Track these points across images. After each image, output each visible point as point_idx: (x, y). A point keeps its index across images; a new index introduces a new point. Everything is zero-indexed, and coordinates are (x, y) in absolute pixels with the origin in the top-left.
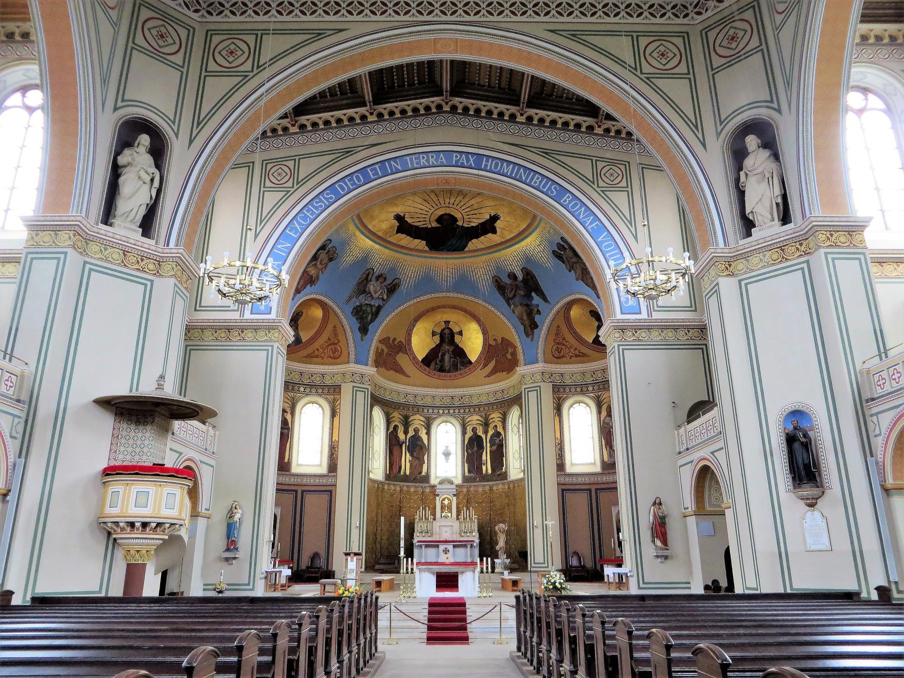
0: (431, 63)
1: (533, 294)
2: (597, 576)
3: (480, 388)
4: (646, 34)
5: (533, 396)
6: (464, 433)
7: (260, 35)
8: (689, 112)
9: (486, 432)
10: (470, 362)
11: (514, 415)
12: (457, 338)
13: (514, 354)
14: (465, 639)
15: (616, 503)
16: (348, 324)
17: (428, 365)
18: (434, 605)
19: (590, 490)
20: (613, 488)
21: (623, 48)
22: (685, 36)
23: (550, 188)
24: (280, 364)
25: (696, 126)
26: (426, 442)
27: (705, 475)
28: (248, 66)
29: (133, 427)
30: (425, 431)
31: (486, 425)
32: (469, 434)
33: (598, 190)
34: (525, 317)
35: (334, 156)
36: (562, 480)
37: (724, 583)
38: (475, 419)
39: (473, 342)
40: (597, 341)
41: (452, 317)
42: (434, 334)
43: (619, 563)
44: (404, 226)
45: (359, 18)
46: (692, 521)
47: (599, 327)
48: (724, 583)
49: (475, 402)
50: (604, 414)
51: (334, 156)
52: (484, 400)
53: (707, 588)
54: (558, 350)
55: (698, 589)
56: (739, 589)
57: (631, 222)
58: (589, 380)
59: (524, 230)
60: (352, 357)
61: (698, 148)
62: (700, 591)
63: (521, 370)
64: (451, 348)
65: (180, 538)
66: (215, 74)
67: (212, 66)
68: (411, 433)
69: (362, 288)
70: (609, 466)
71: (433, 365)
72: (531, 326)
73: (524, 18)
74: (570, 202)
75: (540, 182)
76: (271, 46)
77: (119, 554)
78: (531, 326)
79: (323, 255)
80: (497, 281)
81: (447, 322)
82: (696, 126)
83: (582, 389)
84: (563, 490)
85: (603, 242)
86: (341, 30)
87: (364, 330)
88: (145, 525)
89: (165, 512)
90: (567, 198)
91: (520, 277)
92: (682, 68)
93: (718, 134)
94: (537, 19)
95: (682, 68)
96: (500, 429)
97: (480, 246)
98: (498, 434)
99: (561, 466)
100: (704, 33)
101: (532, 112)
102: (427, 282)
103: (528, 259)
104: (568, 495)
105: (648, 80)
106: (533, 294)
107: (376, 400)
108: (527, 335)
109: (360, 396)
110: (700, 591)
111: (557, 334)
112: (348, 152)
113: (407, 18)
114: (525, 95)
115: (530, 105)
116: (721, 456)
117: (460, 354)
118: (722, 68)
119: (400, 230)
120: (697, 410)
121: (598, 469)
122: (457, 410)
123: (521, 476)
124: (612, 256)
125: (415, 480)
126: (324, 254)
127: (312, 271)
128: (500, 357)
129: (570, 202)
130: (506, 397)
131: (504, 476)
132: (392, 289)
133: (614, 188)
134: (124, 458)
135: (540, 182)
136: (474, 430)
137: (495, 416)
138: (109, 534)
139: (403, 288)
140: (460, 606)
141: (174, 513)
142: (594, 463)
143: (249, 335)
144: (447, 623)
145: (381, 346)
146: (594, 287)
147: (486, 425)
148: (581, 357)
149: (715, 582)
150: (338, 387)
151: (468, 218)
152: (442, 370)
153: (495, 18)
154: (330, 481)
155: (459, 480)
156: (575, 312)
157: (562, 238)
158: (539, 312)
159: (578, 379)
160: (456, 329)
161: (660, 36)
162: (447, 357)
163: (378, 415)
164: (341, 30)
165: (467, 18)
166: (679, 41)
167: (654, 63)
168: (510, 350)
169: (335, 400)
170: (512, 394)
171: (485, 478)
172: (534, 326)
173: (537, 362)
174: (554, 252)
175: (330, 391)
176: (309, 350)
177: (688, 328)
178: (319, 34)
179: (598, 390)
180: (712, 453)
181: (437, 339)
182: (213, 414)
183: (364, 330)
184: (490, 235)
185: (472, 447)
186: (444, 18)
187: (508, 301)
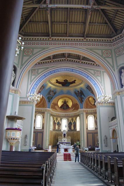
0: (63, 53)
2: (94, 150)
3: (72, 113)
4: (104, 49)
5: (82, 115)
6: (68, 122)
7: (33, 48)
8: (112, 64)
9: (72, 121)
10: (69, 108)
11: (78, 118)
12: (67, 103)
13: (78, 106)
14: (71, 160)
15: (98, 136)
16: (47, 100)
17: (61, 108)
18: (65, 155)
19: (93, 133)
20: (97, 133)
21: (99, 52)
22: (111, 50)
24: (34, 108)
25: (113, 67)
26: (60, 123)
27: (114, 131)
28: (31, 55)
29: (10, 121)
30: (60, 121)
31: (72, 120)
32: (69, 122)
34: (80, 99)
35: (44, 69)
36: (87, 131)
37: (117, 151)
38: (70, 119)
39: (70, 104)
40: (94, 104)
41: (67, 99)
42: (62, 102)
43: (98, 147)
44: (57, 82)
45: (51, 46)
46: (112, 139)
47: (95, 102)
48: (117, 151)
49: (70, 115)
50: (96, 118)
51: (44, 69)
52: (72, 115)
53: (114, 152)
54: (87, 106)
55: (112, 151)
56: (119, 152)
57: (101, 82)
58: (93, 112)
60: (47, 106)
61: (113, 71)
62: (113, 152)
63: (80, 110)
64: (66, 105)
65: (19, 141)
66: (25, 56)
67: (25, 54)
68: (58, 121)
69: (49, 93)
70: (96, 129)
71: (62, 108)
72: (82, 101)
76: (35, 51)
77: (9, 144)
78: (82, 101)
79: (42, 87)
81: (65, 100)
82: (113, 67)
83: (91, 114)
84: (87, 133)
86: (48, 48)
87: (49, 101)
88: (14, 139)
89: (17, 136)
91: (80, 92)
92: (110, 56)
93: (117, 69)
94: (84, 46)
95: (110, 56)
96: (75, 121)
97: (72, 86)
98: (75, 122)
99: (87, 129)
100: (115, 49)
101: (82, 61)
102: (62, 92)
103: (81, 88)
104: (88, 134)
105: (104, 58)
107: (51, 115)
108: (81, 103)
109: (48, 114)
110: (113, 152)
111: (87, 103)
112: (48, 68)
113: (60, 46)
115: (82, 60)
116: (117, 128)
117: (68, 106)
118: (117, 57)
119: (57, 82)
120: (113, 118)
121: (94, 129)
122: (67, 117)
123: (79, 130)
125: (58, 131)
126: (43, 87)
127: (40, 90)
128: (75, 107)
130: (77, 114)
131: (76, 130)
132: (55, 93)
133: (98, 76)
134: (9, 127)
136: (70, 121)
137: (74, 118)
138: (7, 140)
139: (57, 94)
140: (69, 155)
141: (19, 137)
142: (93, 128)
143: (29, 103)
144: (67, 157)
145: (53, 104)
146: (94, 94)
147: (72, 120)
148: (91, 107)
149: (115, 151)
150: (44, 112)
151: (70, 80)
152: (64, 109)
154: (43, 131)
155: (67, 131)
156: (90, 99)
157: (88, 85)
159: (91, 112)
160: (67, 101)
161: (107, 50)
162: (65, 106)
163: (51, 118)
164: (48, 48)
166: (110, 51)
167: (105, 55)
168: (77, 105)
169: (43, 115)
170: (78, 114)
171: (72, 130)
172: (82, 101)
173: (83, 108)
174: (86, 87)
175: (42, 113)
176: (39, 105)
177: (112, 103)
178: (44, 49)
179: (94, 114)
180: (115, 127)
181: (63, 103)
182: (25, 119)
183: (49, 101)
184: (74, 84)
185: (70, 125)
187: (77, 96)
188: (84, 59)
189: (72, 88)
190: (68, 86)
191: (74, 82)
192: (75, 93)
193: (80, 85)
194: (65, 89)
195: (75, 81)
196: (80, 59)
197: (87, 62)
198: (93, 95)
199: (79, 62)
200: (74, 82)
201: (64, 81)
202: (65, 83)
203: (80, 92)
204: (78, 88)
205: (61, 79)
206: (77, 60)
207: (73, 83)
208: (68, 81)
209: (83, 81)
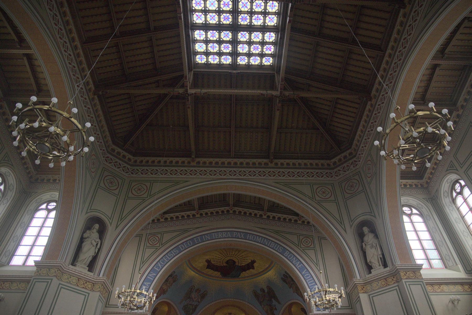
1: (273, 299)
23: (279, 248)
33: (301, 249)
59: (267, 268)
73: (264, 177)
74: (288, 255)
75: (274, 246)
80: (255, 293)
85: (305, 274)
90: (287, 253)
101: (269, 214)
106: (273, 299)
114: (266, 208)
124: (309, 281)
129: (288, 255)
135: (274, 246)
153: (252, 177)
157: (286, 272)
158: (276, 309)
165: (240, 177)
186: (231, 177)
187: (261, 303)
188: (274, 207)
189: (246, 283)
190: (237, 276)
191: (250, 266)
192: (256, 295)
193: (267, 274)
194: (230, 284)
195: (253, 262)
196: (262, 210)
197: (280, 215)
198: (300, 298)
199: (261, 216)
200: (250, 266)
201: (227, 262)
202: (230, 269)
203: (266, 290)
204: (262, 280)
205: (218, 259)
206: (256, 212)
207: (249, 269)
208: (237, 264)
209: (272, 262)
